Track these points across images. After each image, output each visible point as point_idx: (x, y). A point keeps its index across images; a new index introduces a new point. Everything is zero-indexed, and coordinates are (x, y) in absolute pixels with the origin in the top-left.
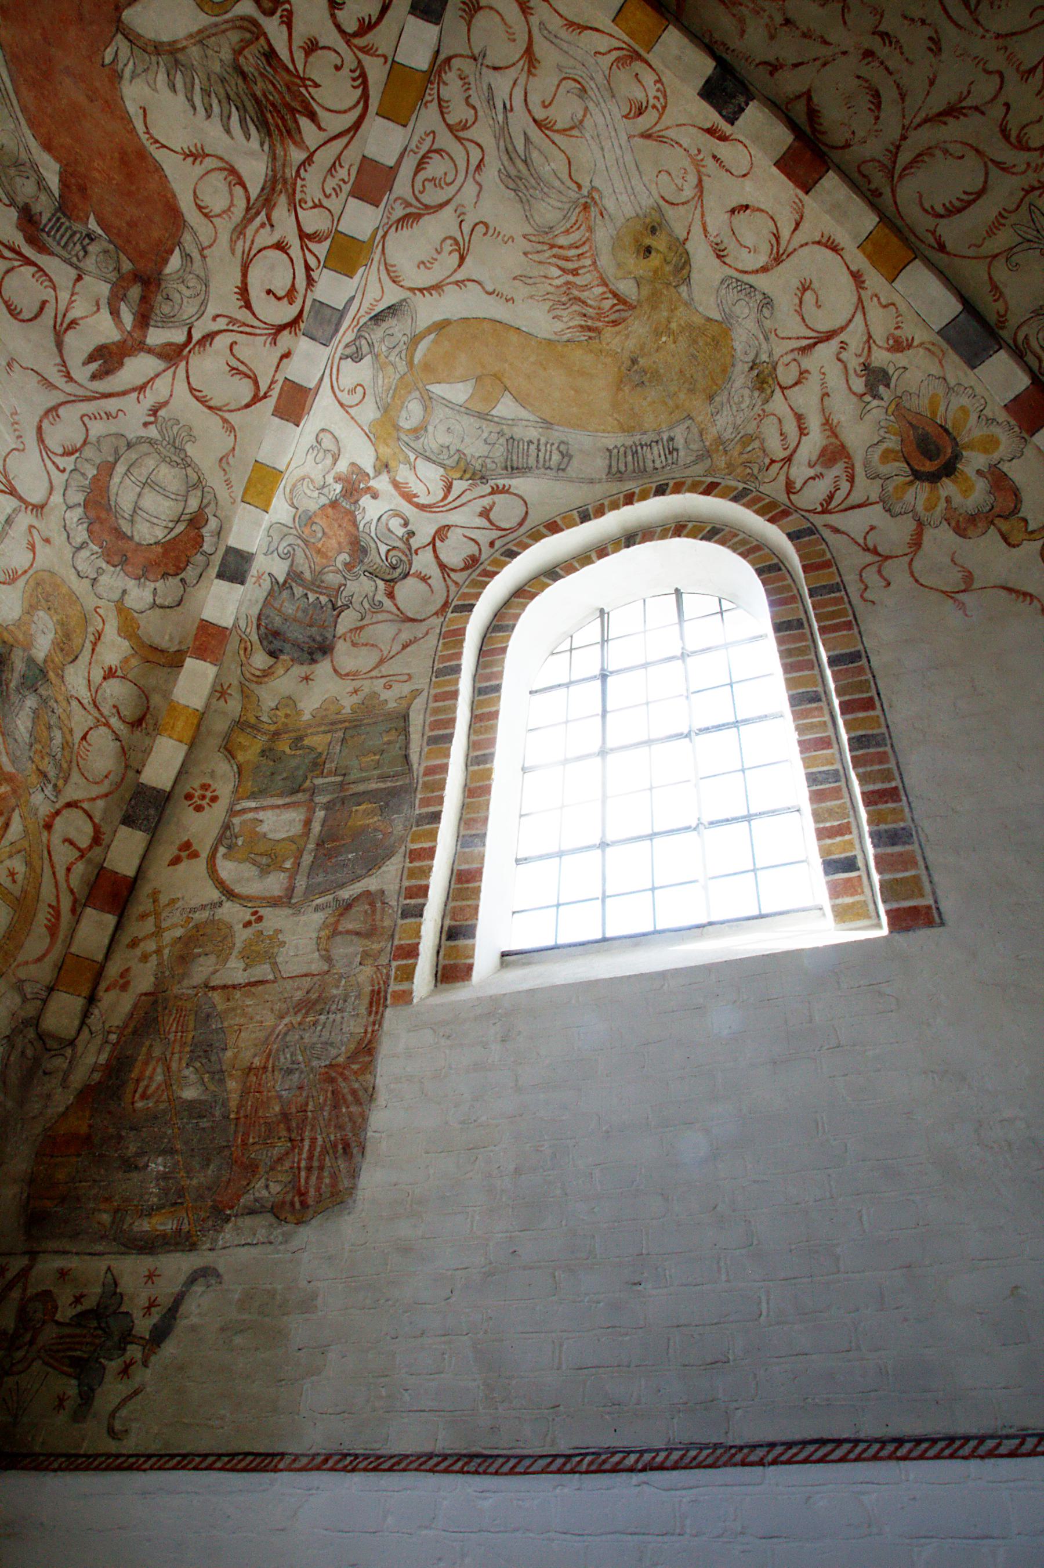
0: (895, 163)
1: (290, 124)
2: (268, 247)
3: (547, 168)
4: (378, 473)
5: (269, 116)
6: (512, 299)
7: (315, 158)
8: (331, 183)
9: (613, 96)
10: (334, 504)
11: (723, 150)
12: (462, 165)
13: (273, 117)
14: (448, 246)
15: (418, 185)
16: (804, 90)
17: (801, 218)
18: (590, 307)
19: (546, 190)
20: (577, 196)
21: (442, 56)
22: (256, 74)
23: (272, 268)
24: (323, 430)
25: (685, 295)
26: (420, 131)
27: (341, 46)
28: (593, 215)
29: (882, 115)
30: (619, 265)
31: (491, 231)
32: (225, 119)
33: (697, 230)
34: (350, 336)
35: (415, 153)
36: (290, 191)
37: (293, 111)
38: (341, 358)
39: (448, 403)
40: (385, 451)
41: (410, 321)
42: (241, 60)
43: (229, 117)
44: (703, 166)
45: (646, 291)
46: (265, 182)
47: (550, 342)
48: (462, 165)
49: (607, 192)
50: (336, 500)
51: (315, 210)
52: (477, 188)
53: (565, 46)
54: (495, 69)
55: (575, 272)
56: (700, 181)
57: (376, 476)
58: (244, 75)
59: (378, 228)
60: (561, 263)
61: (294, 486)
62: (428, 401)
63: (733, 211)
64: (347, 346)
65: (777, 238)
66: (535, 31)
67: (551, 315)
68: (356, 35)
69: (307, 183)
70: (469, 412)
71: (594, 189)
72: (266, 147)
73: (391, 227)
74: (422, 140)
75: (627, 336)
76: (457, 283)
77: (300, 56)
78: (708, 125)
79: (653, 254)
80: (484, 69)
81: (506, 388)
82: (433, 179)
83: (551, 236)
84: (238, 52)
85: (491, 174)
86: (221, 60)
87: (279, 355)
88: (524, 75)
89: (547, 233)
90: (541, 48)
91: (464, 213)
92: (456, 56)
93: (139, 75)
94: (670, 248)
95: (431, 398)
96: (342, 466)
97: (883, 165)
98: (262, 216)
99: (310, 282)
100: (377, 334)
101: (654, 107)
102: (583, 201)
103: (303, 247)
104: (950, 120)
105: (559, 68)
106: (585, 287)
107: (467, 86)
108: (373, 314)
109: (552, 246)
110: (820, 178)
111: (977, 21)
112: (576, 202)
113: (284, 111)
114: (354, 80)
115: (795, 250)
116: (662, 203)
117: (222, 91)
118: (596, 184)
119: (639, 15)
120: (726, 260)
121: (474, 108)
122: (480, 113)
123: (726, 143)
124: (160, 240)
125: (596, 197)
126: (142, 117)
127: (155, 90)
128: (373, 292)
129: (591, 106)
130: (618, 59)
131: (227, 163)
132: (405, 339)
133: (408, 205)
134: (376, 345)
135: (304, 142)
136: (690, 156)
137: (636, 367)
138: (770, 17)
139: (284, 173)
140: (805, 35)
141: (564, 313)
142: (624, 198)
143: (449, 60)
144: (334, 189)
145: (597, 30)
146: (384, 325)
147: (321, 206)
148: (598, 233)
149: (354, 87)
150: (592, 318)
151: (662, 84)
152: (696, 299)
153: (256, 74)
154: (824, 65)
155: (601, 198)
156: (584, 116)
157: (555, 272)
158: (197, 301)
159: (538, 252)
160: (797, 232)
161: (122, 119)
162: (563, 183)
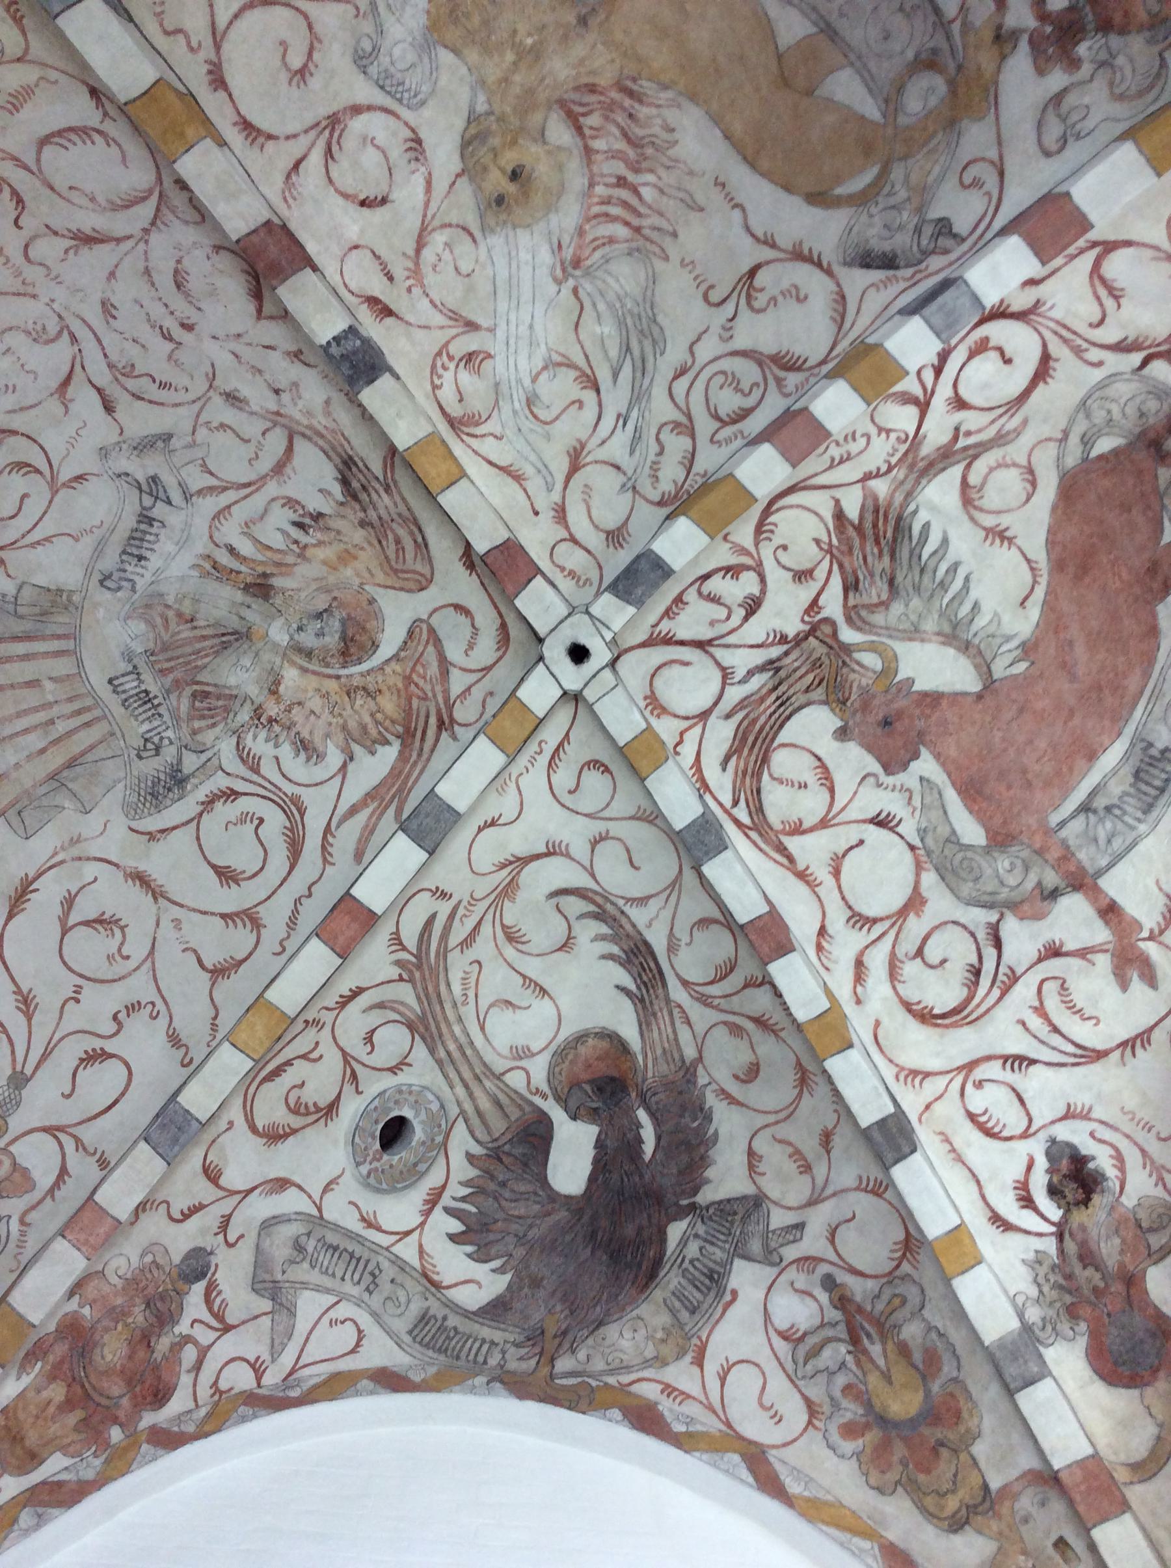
0: (158, 210)
1: (869, 517)
2: (975, 408)
3: (606, 330)
4: (1015, 35)
5: (889, 534)
6: (716, 184)
7: (860, 476)
8: (854, 448)
9: (497, 385)
10: (1105, 26)
11: (377, 286)
12: (700, 385)
13: (885, 533)
14: (761, 300)
15: (757, 394)
16: (263, 322)
17: (288, 176)
18: (618, 126)
19: (618, 305)
20: (582, 281)
21: (666, 511)
22: (877, 578)
23: (986, 386)
24: (1047, 154)
25: (481, 98)
26: (726, 451)
27: (769, 565)
28: (571, 250)
29: (172, 264)
30: (560, 168)
31: (704, 287)
32: (941, 552)
33: (440, 186)
34: (935, 262)
35: (741, 432)
36: (910, 456)
37: (859, 529)
38: (963, 240)
39: (869, 81)
40: (985, 59)
41: (855, 229)
42: (884, 596)
43: (935, 552)
44: (408, 269)
45: (536, 118)
46: (935, 475)
47: (693, 98)
48: (700, 385)
49: (543, 274)
50: (1097, 31)
51: (890, 426)
52: (695, 348)
53: (533, 457)
54: (618, 468)
55: (621, 182)
56: (418, 251)
57: (1023, 31)
58: (891, 582)
59: (826, 376)
60: (634, 201)
61: (1141, 94)
62: (892, 101)
63: (384, 201)
64: (946, 252)
65: (329, 153)
66: (559, 486)
67: (676, 135)
68: (748, 568)
69: (884, 456)
70: (846, 49)
71: (558, 282)
72: (912, 507)
73: (811, 368)
74: (728, 441)
75: (582, 62)
76: (773, 246)
77: (821, 573)
78: (389, 321)
79: (509, 169)
80: (630, 473)
81: (780, 57)
82: (737, 390)
83: (634, 245)
84: (885, 605)
85: (675, 354)
86: (907, 605)
87: (1042, 287)
88: (591, 445)
89: (638, 250)
90: (560, 466)
91: (724, 328)
92: (652, 503)
93: (1003, 636)
94: (485, 169)
95: (886, 101)
96: (1057, 79)
97: (173, 212)
98: (961, 443)
99: (944, 357)
100: (902, 241)
101: (451, 358)
102: (578, 273)
103: (930, 395)
104: (88, 231)
105: (548, 437)
106: (615, 155)
107: (655, 468)
108: (891, 273)
109: (638, 230)
110: (248, 234)
111: (60, 316)
112: (587, 273)
113: (869, 531)
114: (772, 532)
115: (306, 132)
116: (478, 234)
117: (926, 579)
118: (553, 288)
119: (433, 473)
120: (409, 134)
121: (658, 439)
122: (654, 431)
123: (370, 293)
124: (1105, 474)
125: (559, 273)
126: (1031, 599)
127: (996, 614)
128: (875, 302)
129: (527, 382)
130: (477, 424)
131: (968, 513)
132: (874, 210)
133: (779, 382)
134: (911, 226)
135: (865, 498)
136: (423, 286)
137: (584, 11)
138: (295, 404)
139: (906, 477)
140: (260, 371)
141: (656, 130)
142: (524, 256)
143: (660, 504)
144: (854, 439)
145: (490, 463)
146: (887, 246)
147: (880, 430)
148: (573, 224)
149: (776, 525)
150: (624, 109)
151: (432, 382)
152: (467, 89)
153: (877, 578)
154: (239, 335)
155: (553, 267)
156: (539, 374)
157: (646, 192)
158: (1110, 392)
159: (659, 229)
160: (299, 156)
161: (1052, 609)
162: (594, 305)
